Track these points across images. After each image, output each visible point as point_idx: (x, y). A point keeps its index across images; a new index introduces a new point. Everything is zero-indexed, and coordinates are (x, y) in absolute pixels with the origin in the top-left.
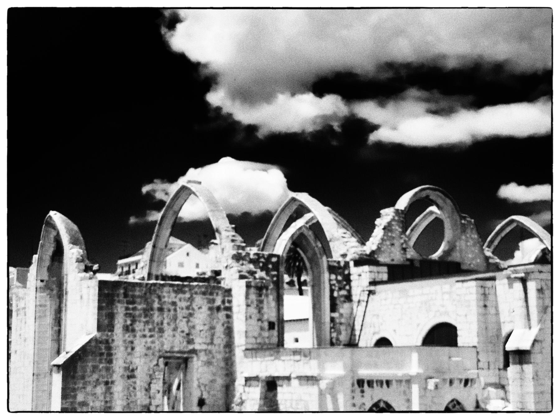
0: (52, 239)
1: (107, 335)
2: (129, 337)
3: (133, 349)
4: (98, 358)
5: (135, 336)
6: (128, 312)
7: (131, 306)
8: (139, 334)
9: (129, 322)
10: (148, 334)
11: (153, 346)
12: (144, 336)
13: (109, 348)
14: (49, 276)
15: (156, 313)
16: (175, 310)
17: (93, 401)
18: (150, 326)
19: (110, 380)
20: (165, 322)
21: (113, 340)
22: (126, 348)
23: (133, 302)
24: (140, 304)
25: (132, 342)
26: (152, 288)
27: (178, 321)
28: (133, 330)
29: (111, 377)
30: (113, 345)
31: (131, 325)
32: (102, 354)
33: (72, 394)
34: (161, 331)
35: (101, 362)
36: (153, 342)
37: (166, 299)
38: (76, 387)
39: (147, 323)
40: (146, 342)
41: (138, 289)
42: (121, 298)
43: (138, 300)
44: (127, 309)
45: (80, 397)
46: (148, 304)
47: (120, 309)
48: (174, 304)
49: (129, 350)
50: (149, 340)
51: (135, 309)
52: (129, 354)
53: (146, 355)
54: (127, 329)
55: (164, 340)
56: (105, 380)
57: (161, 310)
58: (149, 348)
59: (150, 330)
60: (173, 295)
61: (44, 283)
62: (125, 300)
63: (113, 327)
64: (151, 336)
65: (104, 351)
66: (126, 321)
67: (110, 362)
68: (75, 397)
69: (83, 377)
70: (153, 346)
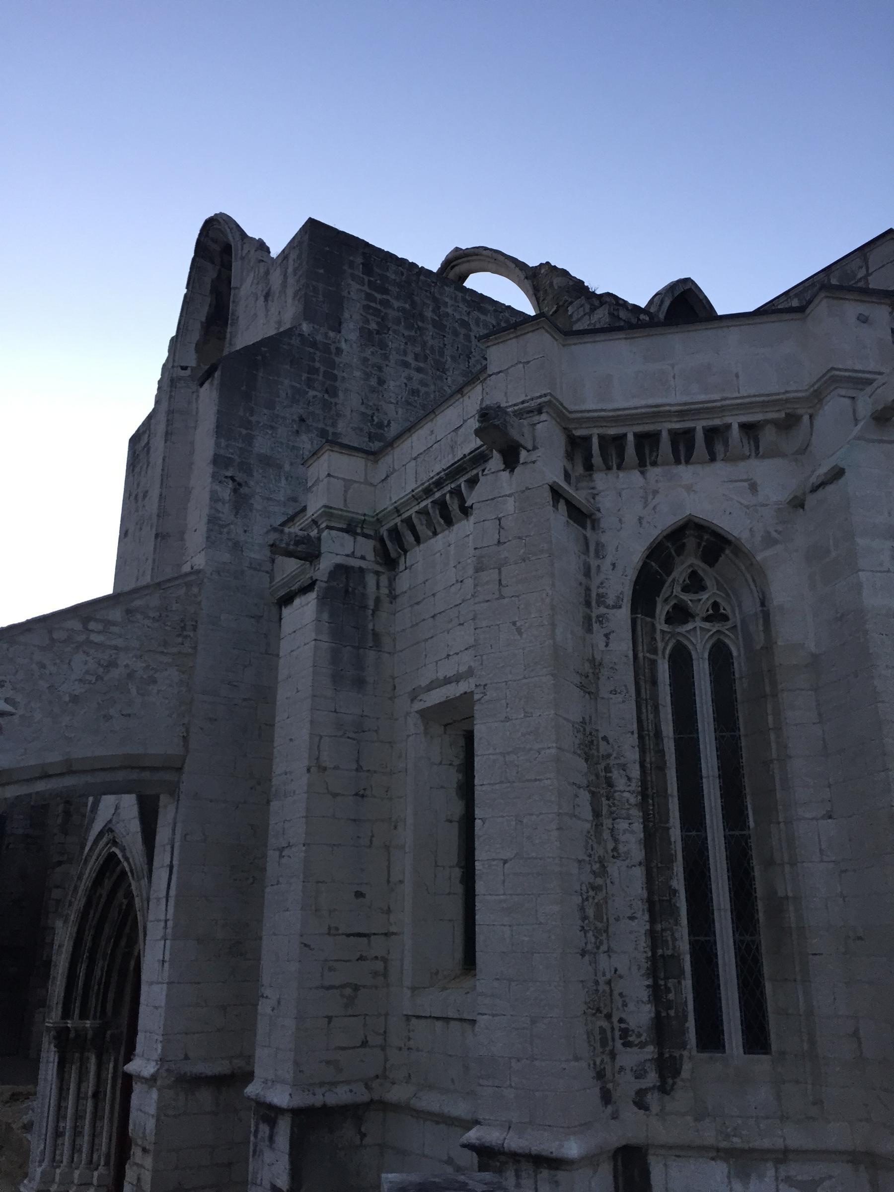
0: (209, 287)
1: (326, 336)
2: (373, 353)
3: (381, 382)
4: (305, 376)
5: (386, 357)
6: (373, 304)
7: (379, 296)
8: (394, 357)
9: (373, 326)
10: (414, 363)
11: (423, 390)
12: (406, 365)
13: (332, 364)
14: (199, 360)
15: (431, 331)
16: (467, 337)
17: (291, 464)
18: (418, 350)
19: (331, 430)
20: (448, 352)
21: (339, 351)
22: (367, 376)
23: (385, 291)
24: (397, 298)
25: (380, 369)
26: (422, 277)
27: (472, 361)
28: (383, 345)
29: (334, 425)
30: (337, 360)
31: (378, 332)
32: (313, 371)
33: (244, 432)
34: (440, 367)
35: (310, 383)
36: (423, 383)
37: (449, 310)
38: (253, 419)
39: (410, 340)
40: (410, 378)
41: (393, 267)
42: (359, 272)
43: (394, 290)
44: (369, 297)
45: (262, 445)
46: (413, 304)
47: (354, 291)
48: (464, 324)
49: (373, 382)
50: (417, 376)
51: (386, 304)
52: (373, 390)
53: (409, 404)
54: (368, 337)
55: (446, 388)
56: (321, 425)
57: (439, 326)
58: (415, 392)
59: (417, 357)
60: (464, 308)
61: (188, 372)
62: (366, 278)
63: (340, 324)
64: (419, 370)
65: (317, 365)
66: (367, 321)
67: (332, 391)
68: (249, 439)
69: (270, 405)
70: (423, 390)
